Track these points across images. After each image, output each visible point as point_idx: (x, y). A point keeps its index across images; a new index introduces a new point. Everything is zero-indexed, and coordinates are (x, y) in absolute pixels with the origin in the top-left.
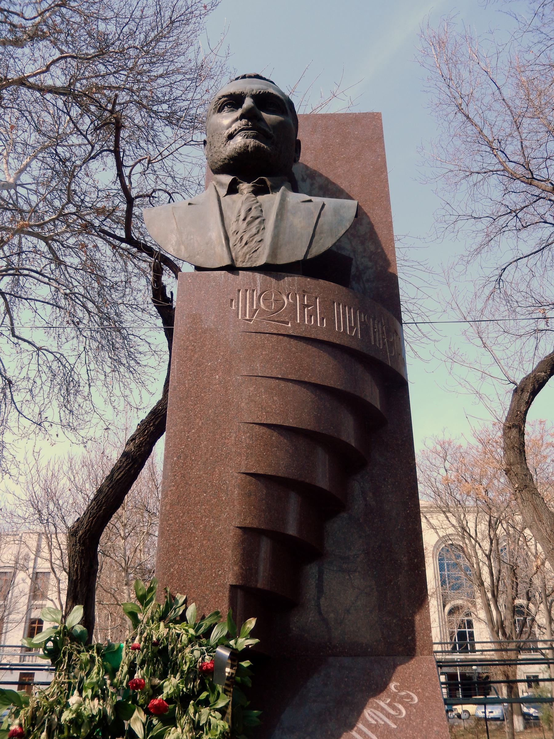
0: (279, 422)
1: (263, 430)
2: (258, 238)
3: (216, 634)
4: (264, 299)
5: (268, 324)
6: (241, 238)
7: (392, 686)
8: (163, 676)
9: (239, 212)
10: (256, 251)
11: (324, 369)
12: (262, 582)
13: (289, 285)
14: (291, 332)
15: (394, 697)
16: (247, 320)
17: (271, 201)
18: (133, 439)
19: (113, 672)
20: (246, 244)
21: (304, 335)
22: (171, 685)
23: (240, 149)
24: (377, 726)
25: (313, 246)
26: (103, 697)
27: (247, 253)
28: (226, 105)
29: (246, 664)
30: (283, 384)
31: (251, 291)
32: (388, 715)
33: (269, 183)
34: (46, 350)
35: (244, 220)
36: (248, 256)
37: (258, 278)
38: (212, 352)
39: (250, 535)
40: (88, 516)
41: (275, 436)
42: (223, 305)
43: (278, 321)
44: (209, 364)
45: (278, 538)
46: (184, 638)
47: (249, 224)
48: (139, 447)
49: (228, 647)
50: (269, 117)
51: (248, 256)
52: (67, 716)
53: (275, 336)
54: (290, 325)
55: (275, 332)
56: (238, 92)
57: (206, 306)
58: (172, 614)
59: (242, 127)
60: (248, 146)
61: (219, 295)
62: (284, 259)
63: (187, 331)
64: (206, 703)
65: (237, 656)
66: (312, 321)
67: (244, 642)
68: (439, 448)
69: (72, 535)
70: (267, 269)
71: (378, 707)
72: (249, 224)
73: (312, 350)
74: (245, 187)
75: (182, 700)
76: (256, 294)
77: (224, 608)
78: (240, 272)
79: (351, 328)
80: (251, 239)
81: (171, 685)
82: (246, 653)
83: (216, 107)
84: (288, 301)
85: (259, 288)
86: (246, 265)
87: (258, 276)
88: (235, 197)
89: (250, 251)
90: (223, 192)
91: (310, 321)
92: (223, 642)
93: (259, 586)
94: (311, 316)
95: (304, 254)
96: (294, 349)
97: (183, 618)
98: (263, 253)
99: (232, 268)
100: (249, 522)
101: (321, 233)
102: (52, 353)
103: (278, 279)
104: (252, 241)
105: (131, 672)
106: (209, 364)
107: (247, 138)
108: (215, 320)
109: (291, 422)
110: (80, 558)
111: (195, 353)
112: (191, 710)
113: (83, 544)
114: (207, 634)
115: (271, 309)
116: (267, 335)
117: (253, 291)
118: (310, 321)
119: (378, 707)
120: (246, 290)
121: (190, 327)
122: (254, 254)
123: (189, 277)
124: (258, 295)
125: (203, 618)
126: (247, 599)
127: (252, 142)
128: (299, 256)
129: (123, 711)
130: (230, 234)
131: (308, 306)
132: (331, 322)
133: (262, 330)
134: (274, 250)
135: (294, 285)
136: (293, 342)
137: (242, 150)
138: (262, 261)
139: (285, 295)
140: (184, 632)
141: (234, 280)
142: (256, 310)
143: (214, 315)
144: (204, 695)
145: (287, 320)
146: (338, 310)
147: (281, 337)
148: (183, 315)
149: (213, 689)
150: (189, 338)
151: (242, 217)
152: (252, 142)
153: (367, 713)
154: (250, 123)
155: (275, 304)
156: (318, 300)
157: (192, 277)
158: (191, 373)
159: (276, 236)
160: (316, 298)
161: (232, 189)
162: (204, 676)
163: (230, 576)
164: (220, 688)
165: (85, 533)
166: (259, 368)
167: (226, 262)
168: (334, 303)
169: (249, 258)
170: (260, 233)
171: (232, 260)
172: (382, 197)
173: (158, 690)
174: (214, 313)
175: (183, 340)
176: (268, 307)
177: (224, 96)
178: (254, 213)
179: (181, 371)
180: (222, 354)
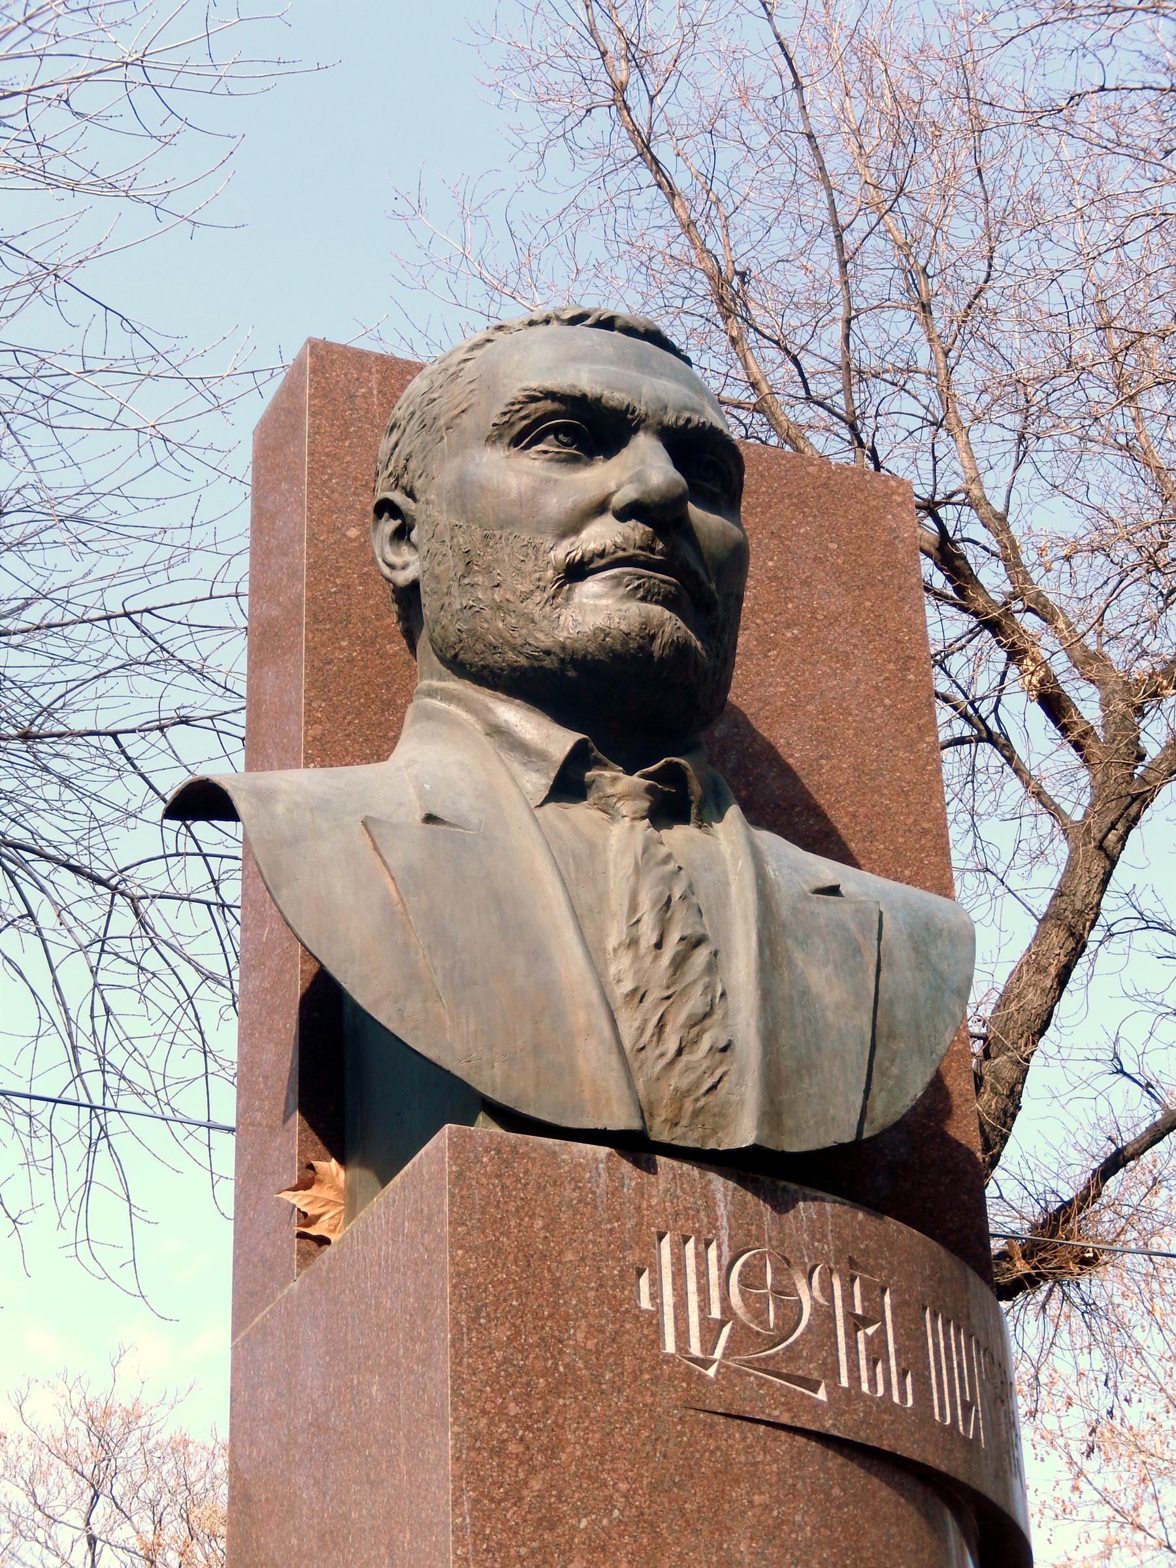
4: (744, 1282)
5: (761, 1386)
6: (661, 1026)
9: (633, 907)
10: (714, 1087)
13: (813, 1237)
14: (828, 1425)
16: (695, 1360)
20: (679, 1052)
21: (863, 1436)
23: (625, 643)
25: (875, 1088)
27: (689, 1091)
28: (555, 430)
31: (702, 1247)
33: (695, 787)
35: (659, 945)
36: (689, 1106)
37: (719, 1196)
38: (589, 1477)
42: (614, 1287)
43: (788, 1378)
44: (584, 1523)
47: (679, 963)
51: (689, 1106)
53: (783, 1435)
54: (822, 1395)
55: (785, 1419)
56: (616, 397)
57: (556, 1283)
59: (631, 551)
60: (653, 637)
61: (594, 1242)
63: (497, 1375)
68: (82, 1441)
74: (621, 785)
76: (719, 1257)
78: (661, 1160)
80: (696, 1029)
83: (509, 424)
84: (812, 1298)
85: (724, 1235)
86: (684, 1136)
87: (719, 1185)
89: (697, 1084)
91: (873, 1382)
94: (875, 1363)
95: (855, 1118)
96: (836, 1491)
98: (742, 1103)
99: (636, 1146)
101: (892, 1036)
103: (782, 1204)
104: (696, 1042)
106: (584, 1523)
107: (643, 599)
108: (590, 1344)
111: (533, 1471)
115: (764, 1323)
116: (762, 1428)
117: (708, 1244)
118: (873, 1382)
120: (686, 1240)
121: (506, 1360)
122: (711, 1098)
123: (487, 1150)
124: (725, 1261)
128: (840, 1128)
131: (864, 1321)
133: (747, 1409)
135: (824, 1236)
136: (835, 1461)
137: (633, 645)
138: (744, 1133)
139: (804, 1271)
141: (640, 1190)
142: (723, 1324)
143: (583, 1324)
145: (815, 1375)
147: (801, 1440)
148: (478, 1311)
150: (502, 1408)
151: (648, 935)
154: (660, 546)
155: (777, 1307)
156: (887, 1299)
157: (498, 1152)
158: (523, 1551)
159: (769, 1037)
160: (883, 1291)
168: (925, 1309)
169: (696, 1113)
170: (718, 1014)
171: (643, 1111)
172: (925, 832)
174: (585, 1316)
175: (484, 1412)
177: (550, 395)
179: (487, 1538)
180: (623, 1486)
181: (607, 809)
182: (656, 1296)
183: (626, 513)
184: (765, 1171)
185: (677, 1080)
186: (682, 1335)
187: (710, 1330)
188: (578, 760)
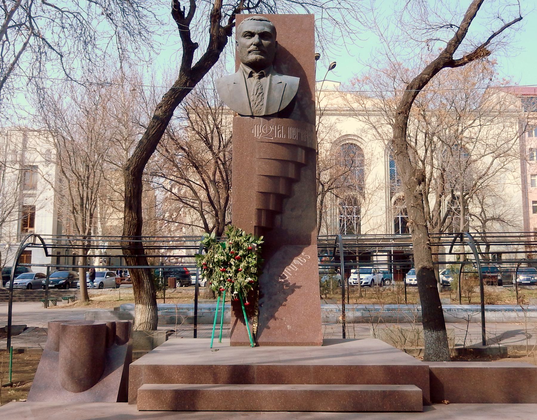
0: (269, 174)
1: (264, 177)
2: (261, 104)
3: (251, 240)
7: (303, 254)
8: (238, 250)
11: (283, 153)
12: (263, 224)
15: (303, 257)
17: (266, 80)
18: (160, 107)
19: (224, 249)
24: (297, 265)
26: (224, 256)
29: (260, 247)
30: (270, 161)
32: (301, 262)
33: (265, 73)
34: (68, 12)
39: (259, 210)
40: (135, 158)
41: (267, 179)
45: (268, 211)
46: (243, 241)
47: (258, 96)
48: (165, 112)
49: (256, 243)
50: (265, 42)
52: (215, 260)
56: (253, 31)
58: (238, 234)
64: (250, 257)
65: (258, 245)
66: (280, 136)
67: (260, 242)
69: (126, 170)
70: (264, 117)
71: (298, 260)
72: (258, 96)
74: (256, 75)
75: (244, 256)
77: (253, 232)
79: (294, 136)
81: (241, 253)
82: (261, 245)
87: (261, 119)
88: (252, 79)
90: (247, 76)
92: (254, 241)
93: (262, 225)
97: (241, 235)
99: (252, 116)
100: (260, 207)
102: (72, 13)
103: (269, 120)
105: (230, 249)
109: (273, 174)
110: (133, 184)
112: (247, 258)
113: (134, 175)
114: (249, 239)
119: (298, 260)
125: (247, 235)
126: (260, 230)
127: (258, 57)
128: (277, 111)
129: (229, 258)
130: (251, 100)
134: (267, 110)
138: (263, 114)
140: (242, 239)
144: (249, 255)
146: (290, 130)
149: (251, 254)
152: (258, 57)
153: (294, 261)
161: (251, 75)
162: (249, 250)
163: (254, 223)
164: (253, 253)
165: (135, 168)
166: (262, 155)
167: (250, 114)
173: (237, 254)
176: (265, 132)
181: (254, 78)
182: (254, 131)
183: (254, 45)
184: (267, 117)
185: (256, 109)
186: (257, 135)
187: (260, 134)
188: (251, 73)
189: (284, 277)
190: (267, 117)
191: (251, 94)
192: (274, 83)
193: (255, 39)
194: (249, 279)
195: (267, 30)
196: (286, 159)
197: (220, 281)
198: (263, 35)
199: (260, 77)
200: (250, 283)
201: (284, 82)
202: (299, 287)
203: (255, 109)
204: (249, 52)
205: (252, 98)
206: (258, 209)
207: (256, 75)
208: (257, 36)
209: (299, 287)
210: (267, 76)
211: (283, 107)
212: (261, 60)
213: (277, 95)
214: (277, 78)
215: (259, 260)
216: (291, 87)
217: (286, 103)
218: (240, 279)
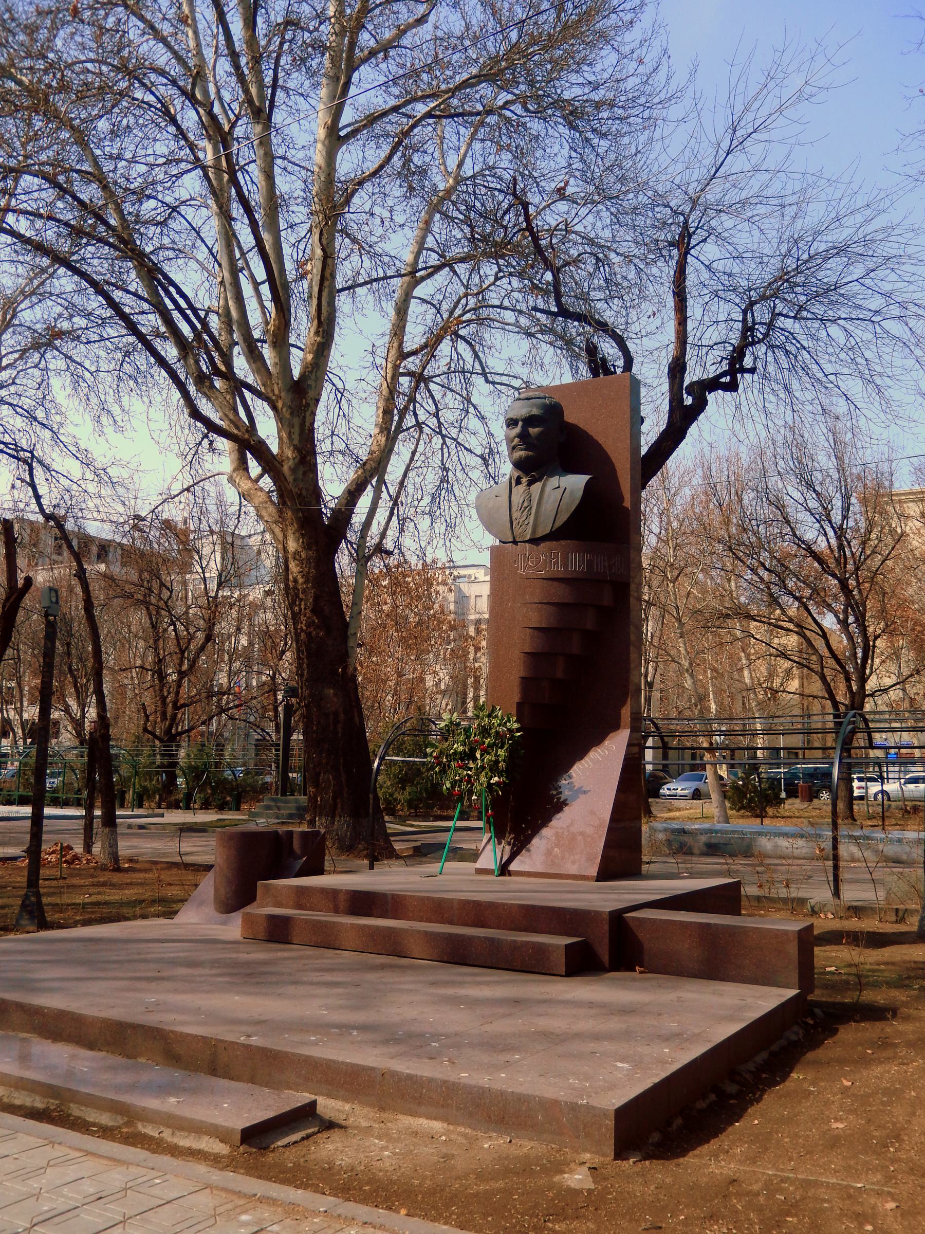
11: (561, 593)
17: (537, 486)
22: (487, 741)
41: (536, 633)
50: (533, 431)
62: (540, 533)
64: (502, 748)
70: (531, 541)
73: (556, 584)
75: (491, 746)
81: (487, 741)
99: (515, 542)
103: (538, 545)
109: (544, 625)
128: (548, 531)
132: (567, 566)
134: (534, 531)
146: (572, 556)
178: (525, 504)
184: (534, 541)
189: (570, 777)
190: (534, 541)
191: (514, 509)
192: (548, 489)
193: (518, 430)
194: (496, 779)
195: (535, 411)
196: (566, 601)
197: (456, 781)
198: (529, 421)
199: (530, 484)
200: (498, 784)
201: (563, 485)
202: (585, 792)
203: (518, 531)
204: (514, 448)
205: (515, 516)
206: (522, 678)
207: (524, 480)
208: (520, 423)
209: (585, 792)
210: (539, 480)
211: (559, 523)
212: (527, 458)
213: (550, 506)
214: (554, 481)
215: (511, 752)
216: (572, 492)
217: (563, 518)
218: (483, 779)
